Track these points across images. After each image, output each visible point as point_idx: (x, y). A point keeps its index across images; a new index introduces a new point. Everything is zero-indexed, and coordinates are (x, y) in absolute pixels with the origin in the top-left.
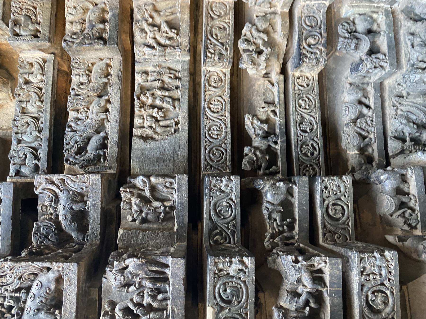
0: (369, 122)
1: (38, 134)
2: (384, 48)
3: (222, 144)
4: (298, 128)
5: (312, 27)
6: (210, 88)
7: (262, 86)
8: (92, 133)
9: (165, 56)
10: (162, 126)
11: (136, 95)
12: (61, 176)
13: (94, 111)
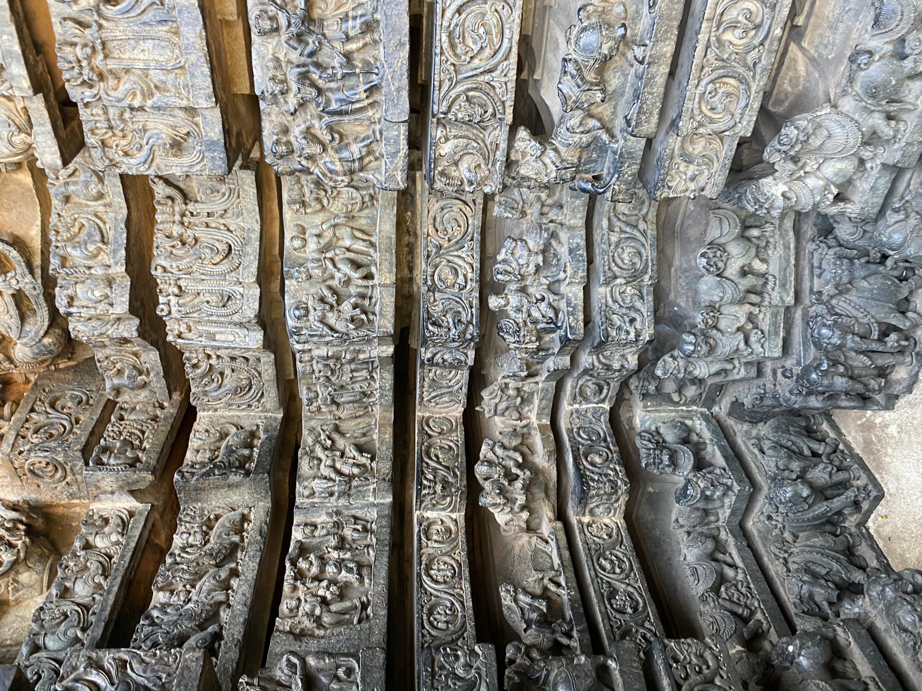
0: (743, 590)
1: (79, 634)
2: (720, 460)
3: (458, 639)
4: (608, 606)
5: (592, 440)
6: (429, 542)
7: (527, 546)
8: (191, 628)
9: (349, 496)
10: (335, 612)
11: (289, 559)
12: (123, 654)
13: (204, 588)
